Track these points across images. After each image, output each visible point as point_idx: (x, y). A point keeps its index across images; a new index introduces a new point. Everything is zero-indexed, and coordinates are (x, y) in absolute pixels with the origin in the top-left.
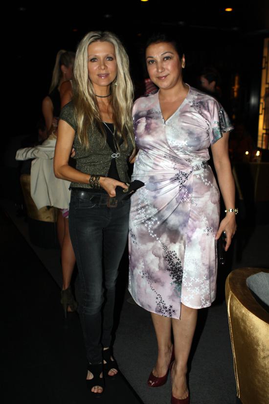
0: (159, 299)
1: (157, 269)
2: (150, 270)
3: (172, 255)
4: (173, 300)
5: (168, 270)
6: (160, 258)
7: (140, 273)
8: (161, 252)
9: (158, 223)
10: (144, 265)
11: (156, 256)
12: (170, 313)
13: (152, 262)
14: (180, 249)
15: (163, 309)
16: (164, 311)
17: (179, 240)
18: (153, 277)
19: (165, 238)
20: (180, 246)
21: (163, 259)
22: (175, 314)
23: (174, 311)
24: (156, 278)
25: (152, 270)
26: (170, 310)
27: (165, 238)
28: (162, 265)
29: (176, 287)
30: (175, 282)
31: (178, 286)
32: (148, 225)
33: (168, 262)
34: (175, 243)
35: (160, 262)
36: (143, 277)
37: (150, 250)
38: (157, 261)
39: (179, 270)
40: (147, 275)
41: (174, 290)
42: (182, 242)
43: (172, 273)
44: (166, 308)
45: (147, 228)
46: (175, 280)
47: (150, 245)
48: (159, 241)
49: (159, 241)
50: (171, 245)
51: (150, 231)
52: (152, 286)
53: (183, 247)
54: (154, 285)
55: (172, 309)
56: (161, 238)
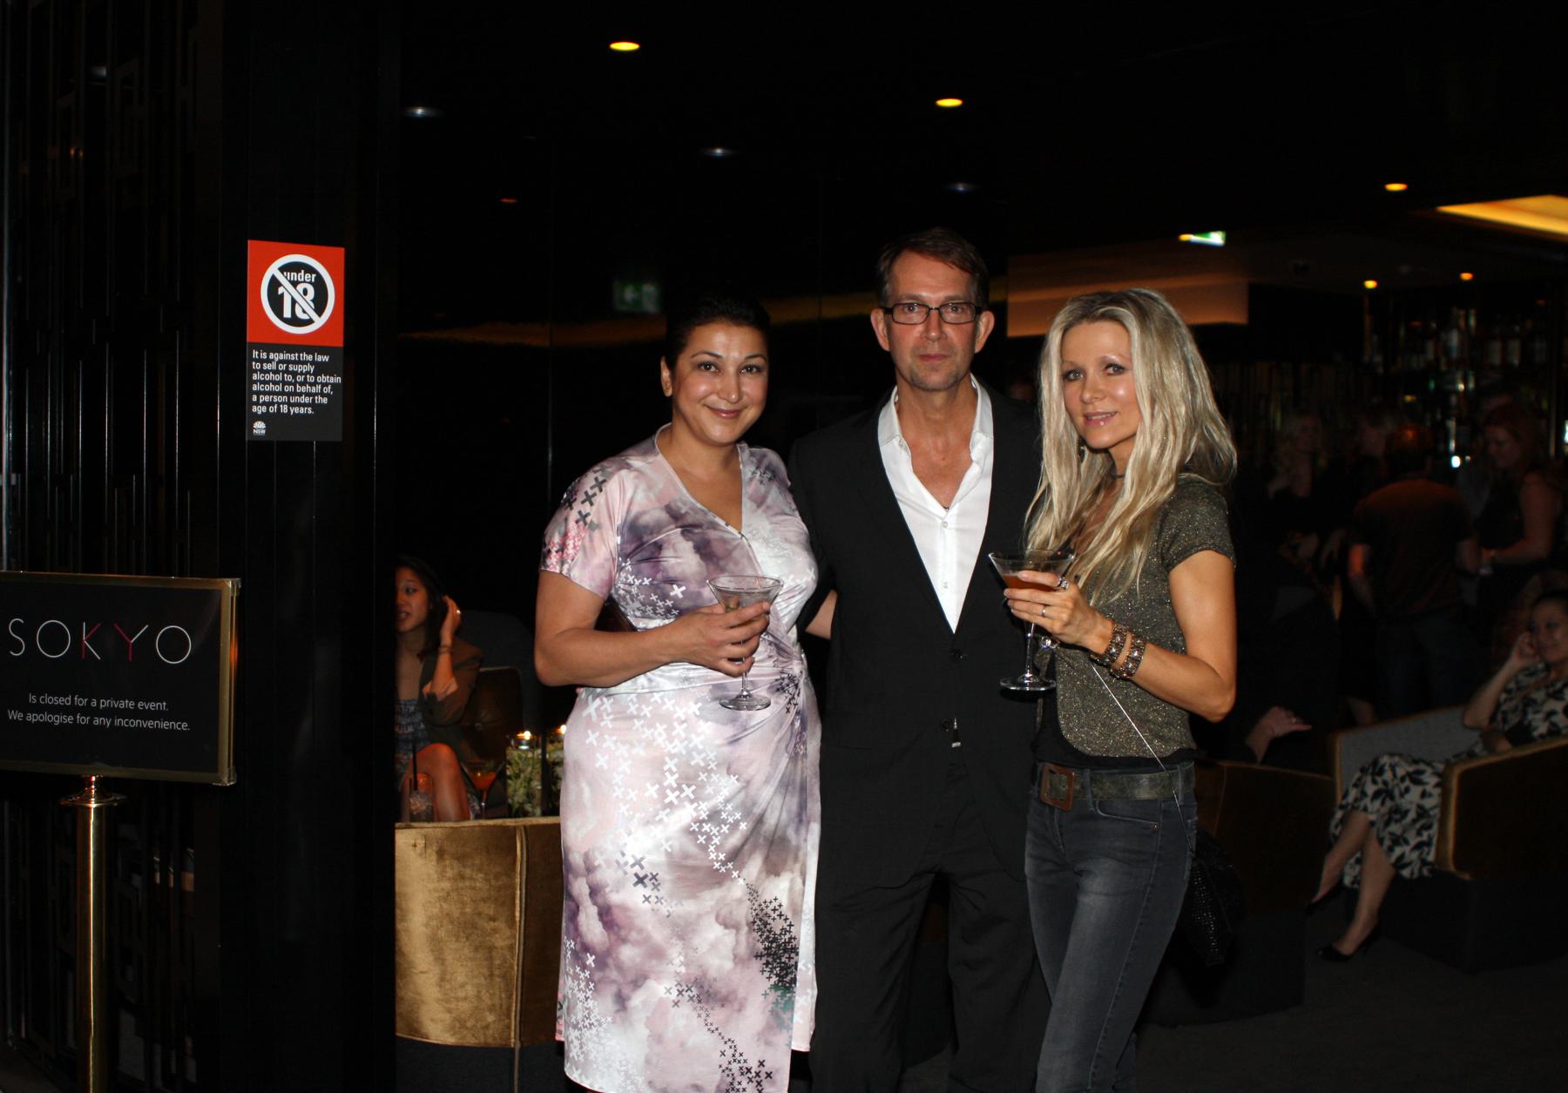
0: (729, 1053)
1: (729, 965)
2: (704, 974)
3: (769, 911)
4: (767, 1043)
5: (758, 956)
6: (737, 927)
7: (669, 991)
8: (743, 913)
9: (743, 826)
10: (686, 964)
11: (726, 926)
12: (759, 1083)
13: (714, 946)
14: (791, 889)
15: (738, 1079)
16: (744, 1084)
17: (790, 862)
18: (716, 993)
19: (754, 865)
20: (792, 880)
21: (745, 929)
22: (773, 1084)
23: (769, 1075)
24: (724, 991)
25: (712, 973)
26: (758, 1074)
27: (754, 865)
28: (743, 950)
29: (776, 1003)
30: (775, 987)
31: (783, 996)
32: (709, 839)
33: (756, 935)
34: (777, 874)
35: (737, 942)
36: (676, 1004)
37: (708, 913)
38: (728, 938)
39: (785, 950)
40: (695, 991)
41: (772, 1011)
42: (798, 866)
43: (767, 964)
44: (749, 1070)
45: (704, 848)
46: (774, 979)
47: (710, 898)
48: (741, 881)
49: (741, 881)
50: (767, 883)
51: (713, 856)
52: (709, 1020)
53: (799, 881)
54: (718, 1015)
55: (764, 1070)
56: (745, 872)
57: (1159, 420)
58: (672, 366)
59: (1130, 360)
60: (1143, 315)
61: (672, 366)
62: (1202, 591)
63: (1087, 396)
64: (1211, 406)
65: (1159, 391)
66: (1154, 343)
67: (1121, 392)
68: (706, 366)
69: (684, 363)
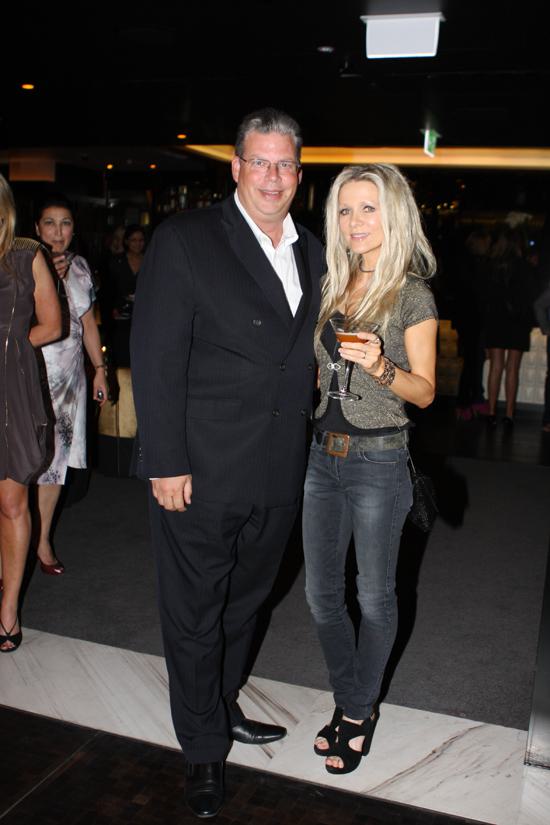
57: (394, 242)
58: (38, 224)
59: (378, 204)
60: (386, 179)
61: (38, 224)
62: (421, 341)
63: (353, 224)
64: (421, 233)
65: (393, 223)
66: (392, 195)
67: (372, 222)
68: (49, 223)
69: (42, 223)
